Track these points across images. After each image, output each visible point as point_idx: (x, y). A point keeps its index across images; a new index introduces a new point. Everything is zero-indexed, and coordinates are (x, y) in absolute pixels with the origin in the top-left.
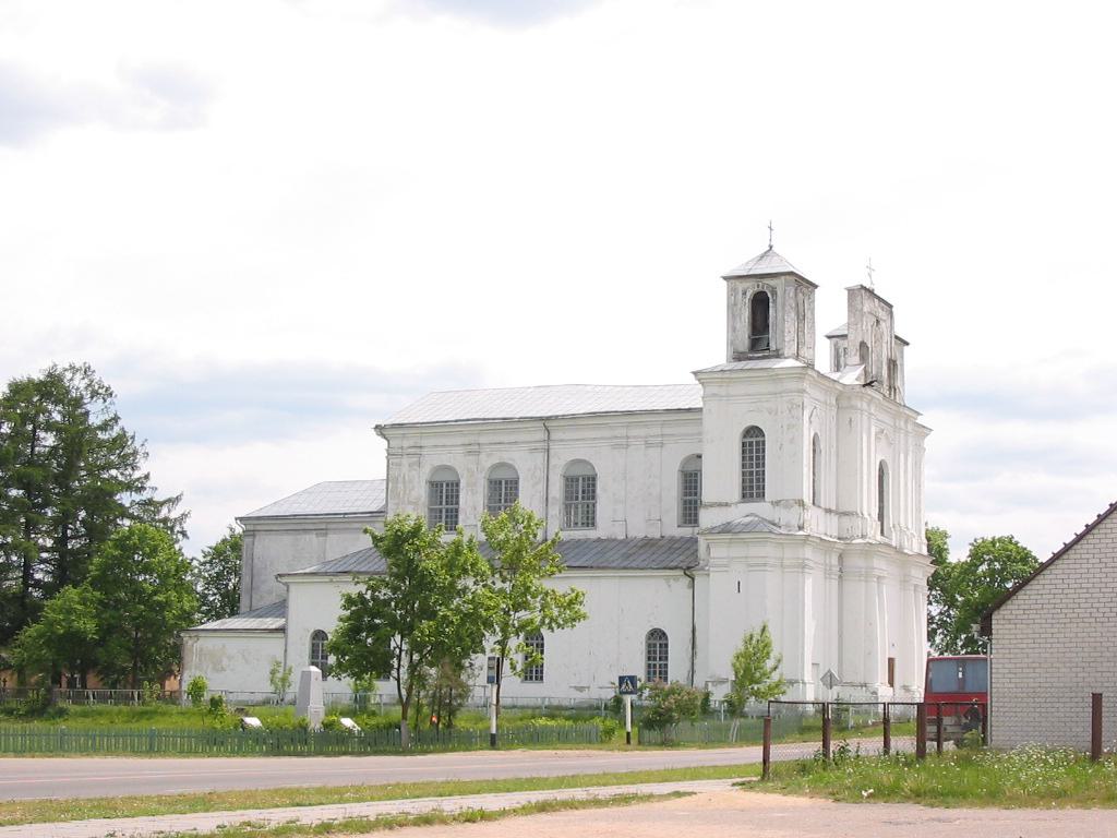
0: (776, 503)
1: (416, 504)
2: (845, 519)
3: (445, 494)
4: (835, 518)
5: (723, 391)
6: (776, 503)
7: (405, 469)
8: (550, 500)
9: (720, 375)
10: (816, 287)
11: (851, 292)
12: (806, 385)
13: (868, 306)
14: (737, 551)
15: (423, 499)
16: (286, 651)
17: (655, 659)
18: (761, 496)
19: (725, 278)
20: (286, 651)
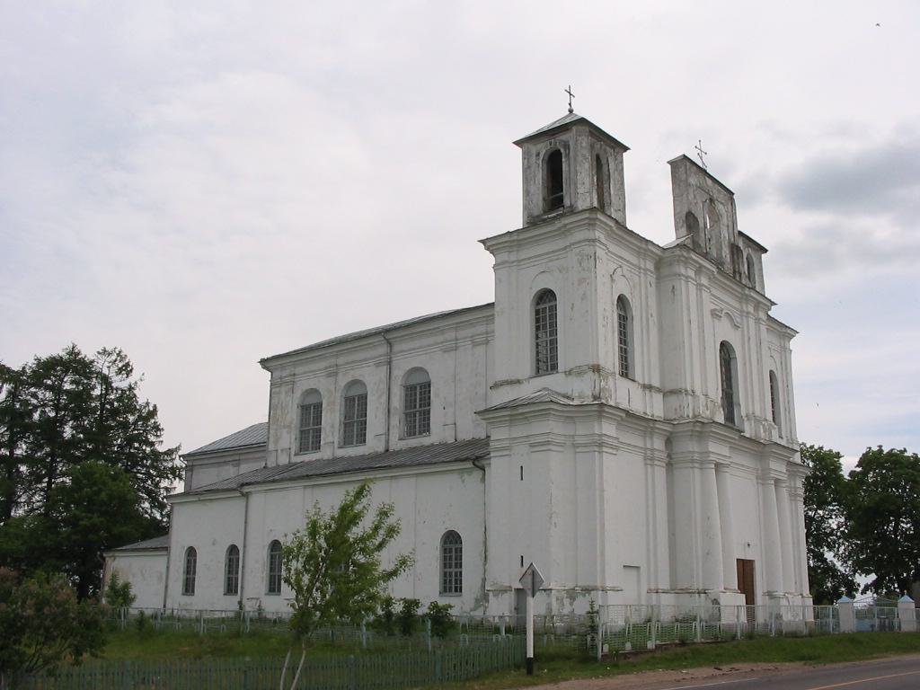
0: (569, 373)
1: (289, 427)
2: (673, 400)
3: (311, 412)
4: (658, 398)
5: (513, 257)
6: (569, 373)
7: (283, 396)
8: (392, 411)
9: (507, 239)
10: (626, 149)
11: (675, 164)
12: (598, 234)
13: (693, 180)
14: (519, 431)
15: (295, 422)
16: (168, 567)
17: (450, 567)
18: (554, 368)
19: (518, 143)
20: (168, 567)
